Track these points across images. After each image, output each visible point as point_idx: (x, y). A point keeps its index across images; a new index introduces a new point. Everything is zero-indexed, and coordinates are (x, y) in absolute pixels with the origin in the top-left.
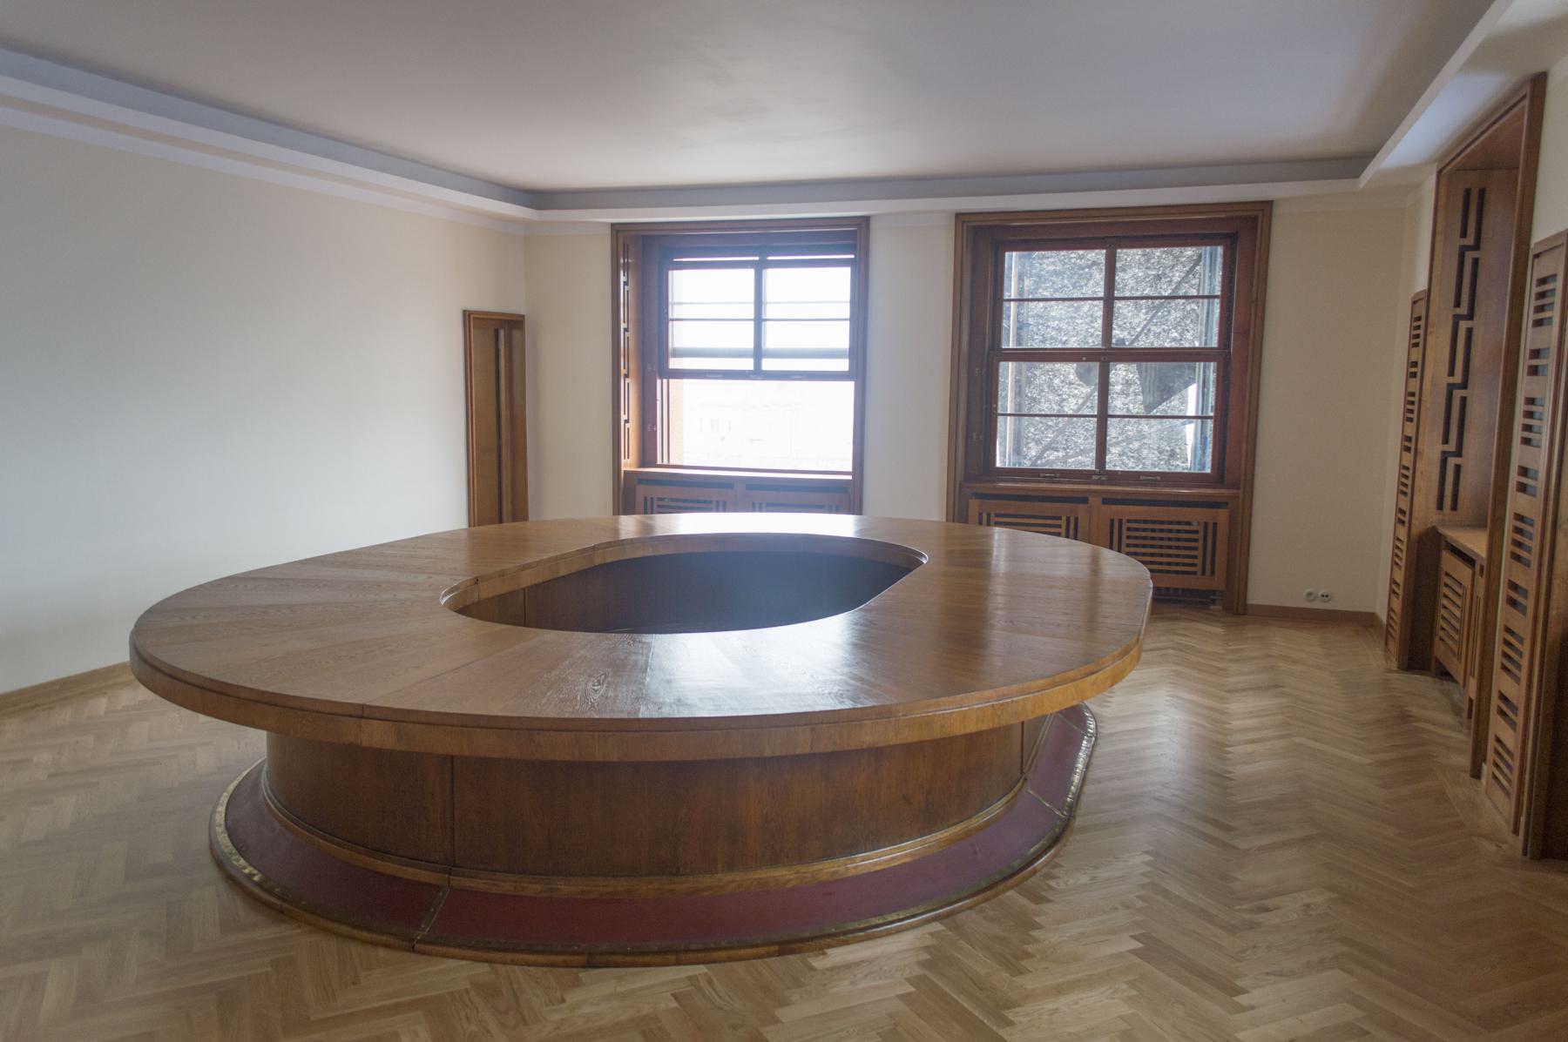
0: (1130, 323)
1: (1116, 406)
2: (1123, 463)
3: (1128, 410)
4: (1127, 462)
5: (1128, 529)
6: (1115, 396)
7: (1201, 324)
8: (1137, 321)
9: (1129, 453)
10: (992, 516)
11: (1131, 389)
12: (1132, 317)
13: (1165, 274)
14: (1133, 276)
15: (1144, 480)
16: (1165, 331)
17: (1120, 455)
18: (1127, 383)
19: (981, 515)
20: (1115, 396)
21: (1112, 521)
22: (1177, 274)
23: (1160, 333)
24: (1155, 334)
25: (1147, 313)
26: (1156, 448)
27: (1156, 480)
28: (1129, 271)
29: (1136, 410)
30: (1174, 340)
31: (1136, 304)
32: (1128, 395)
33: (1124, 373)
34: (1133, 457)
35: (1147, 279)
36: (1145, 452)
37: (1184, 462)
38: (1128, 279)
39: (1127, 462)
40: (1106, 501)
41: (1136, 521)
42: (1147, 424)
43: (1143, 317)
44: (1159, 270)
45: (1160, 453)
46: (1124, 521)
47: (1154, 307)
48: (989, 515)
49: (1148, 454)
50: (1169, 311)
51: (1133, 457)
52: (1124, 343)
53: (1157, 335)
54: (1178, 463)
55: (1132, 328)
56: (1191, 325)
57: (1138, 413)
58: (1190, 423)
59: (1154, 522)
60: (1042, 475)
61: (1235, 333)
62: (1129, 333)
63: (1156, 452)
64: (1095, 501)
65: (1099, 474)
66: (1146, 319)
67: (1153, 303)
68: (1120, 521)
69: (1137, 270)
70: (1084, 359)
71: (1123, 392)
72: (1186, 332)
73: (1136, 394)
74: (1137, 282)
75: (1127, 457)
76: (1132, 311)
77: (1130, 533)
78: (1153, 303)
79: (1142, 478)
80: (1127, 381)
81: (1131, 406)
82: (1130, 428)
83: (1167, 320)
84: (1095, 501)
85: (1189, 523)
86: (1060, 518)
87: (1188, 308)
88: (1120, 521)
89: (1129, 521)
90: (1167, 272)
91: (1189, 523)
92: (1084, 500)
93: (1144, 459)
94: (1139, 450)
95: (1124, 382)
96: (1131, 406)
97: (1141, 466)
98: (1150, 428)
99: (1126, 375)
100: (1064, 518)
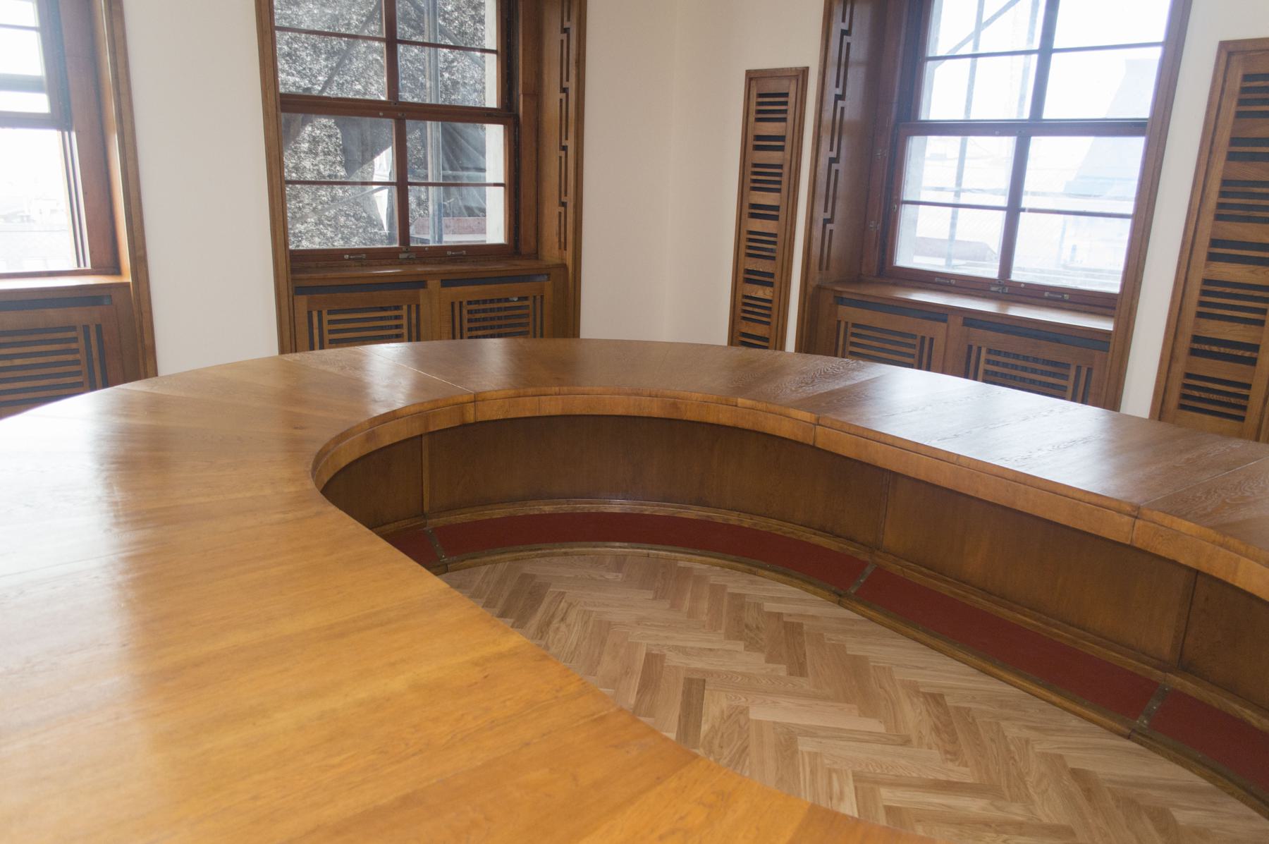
0: (310, 69)
1: (305, 167)
2: (321, 233)
3: (319, 172)
4: (325, 231)
5: (470, 312)
6: (302, 155)
7: (430, 80)
8: (317, 67)
9: (326, 222)
10: (325, 312)
11: (320, 148)
12: (312, 61)
13: (342, 15)
14: (308, 12)
15: (452, 256)
16: (348, 83)
17: (316, 224)
18: (314, 140)
19: (310, 314)
20: (302, 155)
21: (453, 304)
22: (355, 17)
23: (343, 84)
24: (338, 84)
25: (326, 59)
26: (352, 214)
27: (462, 255)
28: (302, 5)
29: (326, 173)
30: (358, 92)
31: (314, 46)
32: (317, 154)
34: (330, 225)
35: (324, 19)
36: (342, 219)
37: (380, 230)
38: (302, 15)
39: (325, 231)
40: (446, 283)
41: (477, 302)
42: (341, 189)
43: (323, 63)
44: (335, 10)
45: (357, 220)
46: (464, 303)
47: (334, 52)
48: (320, 313)
49: (345, 221)
50: (351, 60)
51: (330, 225)
52: (310, 92)
53: (341, 86)
54: (376, 230)
55: (313, 76)
56: (375, 78)
57: (330, 176)
58: (385, 188)
59: (492, 301)
60: (347, 257)
61: (524, 95)
62: (310, 81)
63: (353, 219)
64: (434, 284)
65: (405, 252)
66: (327, 66)
67: (332, 48)
68: (461, 303)
69: (311, 6)
70: (381, 114)
71: (310, 151)
72: (369, 85)
73: (327, 154)
74: (313, 20)
75: (324, 226)
76: (311, 55)
77: (471, 316)
78: (332, 48)
79: (449, 253)
80: (314, 138)
81: (322, 167)
82: (324, 193)
83: (349, 70)
84: (434, 284)
85: (507, 300)
86: (398, 308)
87: (370, 58)
88: (461, 303)
89: (469, 303)
90: (344, 13)
91: (507, 300)
92: (422, 284)
93: (342, 227)
94: (335, 218)
95: (312, 139)
96: (322, 167)
97: (340, 236)
98: (344, 192)
99: (313, 131)
100: (405, 307)
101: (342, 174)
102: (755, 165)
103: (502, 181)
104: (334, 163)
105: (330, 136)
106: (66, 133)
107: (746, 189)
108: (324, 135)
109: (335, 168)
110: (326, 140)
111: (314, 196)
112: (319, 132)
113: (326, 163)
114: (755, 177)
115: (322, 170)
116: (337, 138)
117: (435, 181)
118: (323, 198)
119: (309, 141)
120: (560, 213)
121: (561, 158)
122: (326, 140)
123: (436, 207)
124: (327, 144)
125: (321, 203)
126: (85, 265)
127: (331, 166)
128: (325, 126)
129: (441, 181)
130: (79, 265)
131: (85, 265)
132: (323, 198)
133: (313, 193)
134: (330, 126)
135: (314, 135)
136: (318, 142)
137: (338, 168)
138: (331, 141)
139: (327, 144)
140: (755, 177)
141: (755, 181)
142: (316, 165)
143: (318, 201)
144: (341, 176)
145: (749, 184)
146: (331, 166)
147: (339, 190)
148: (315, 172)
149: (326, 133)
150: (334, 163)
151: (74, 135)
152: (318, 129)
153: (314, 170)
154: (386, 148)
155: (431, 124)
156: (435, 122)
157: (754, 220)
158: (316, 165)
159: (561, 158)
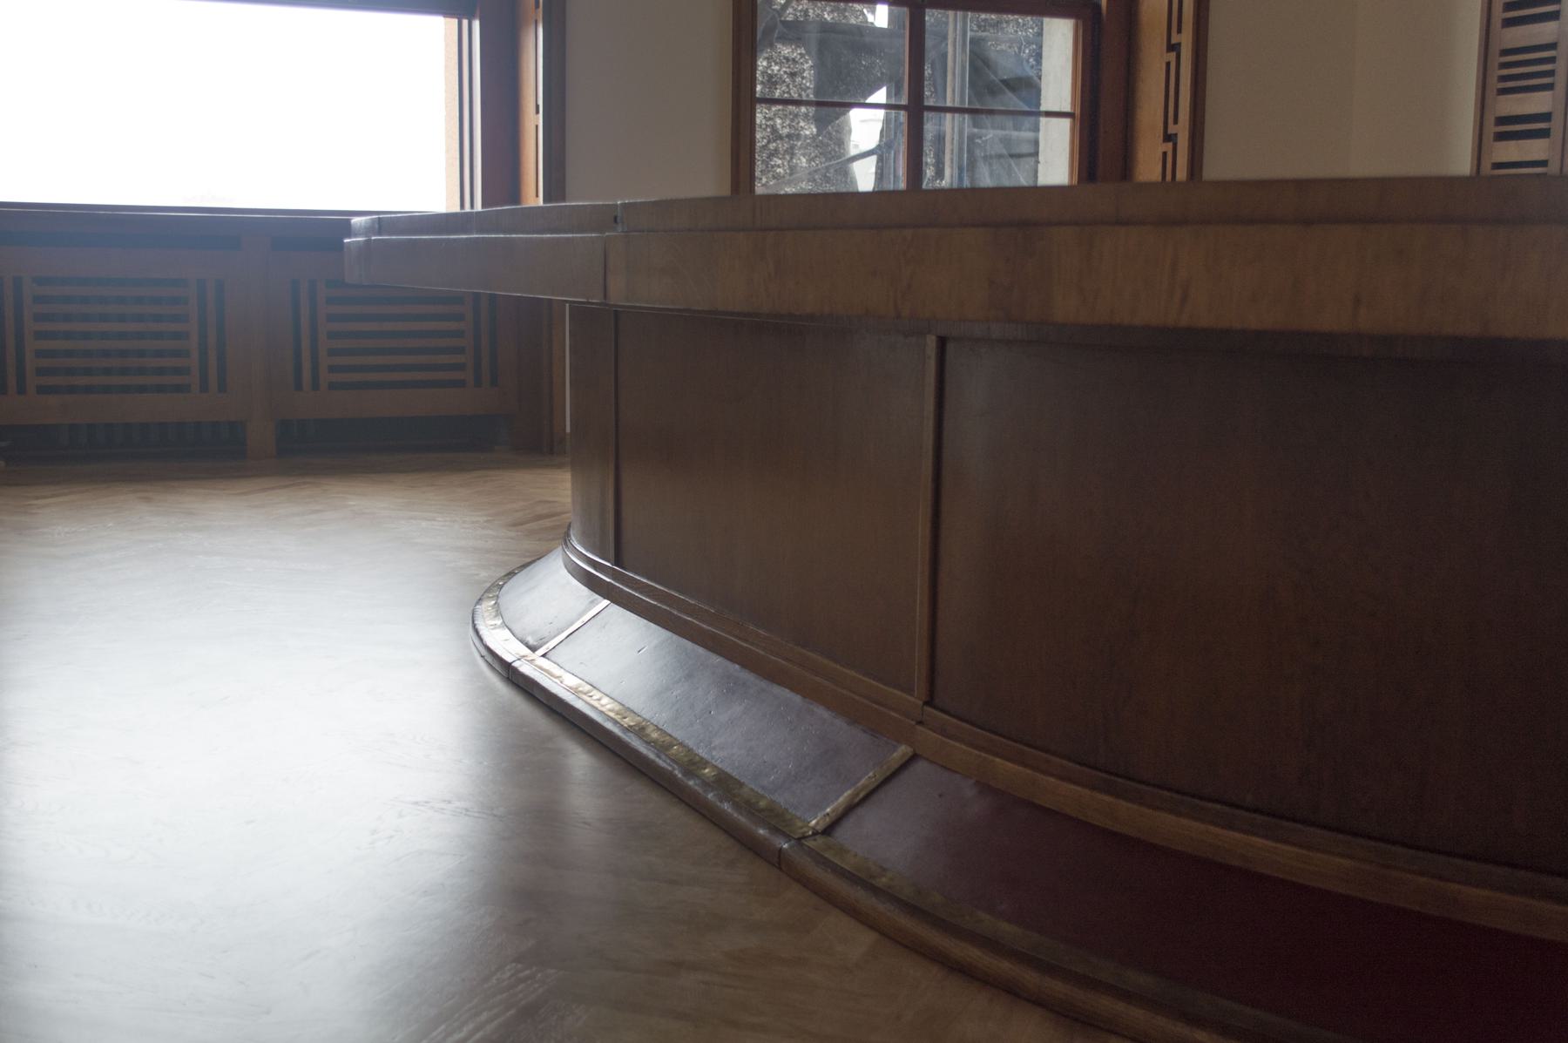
3: (774, 130)
18: (768, 81)
29: (786, 131)
33: (765, 63)
80: (771, 77)
81: (779, 121)
82: (780, 162)
95: (766, 78)
96: (779, 121)
101: (808, 133)
102: (1505, 52)
103: (1067, 108)
104: (796, 116)
105: (793, 75)
106: (465, 22)
107: (1491, 93)
108: (785, 72)
109: (799, 122)
110: (787, 80)
111: (764, 167)
112: (777, 68)
113: (786, 115)
114: (1505, 72)
115: (779, 126)
116: (803, 78)
117: (957, 105)
118: (778, 170)
119: (762, 83)
120: (1165, 154)
121: (1168, 64)
122: (787, 80)
123: (956, 171)
124: (788, 86)
125: (774, 177)
126: (472, 206)
127: (792, 120)
128: (787, 59)
129: (967, 106)
130: (462, 206)
131: (472, 206)
132: (778, 170)
133: (763, 161)
134: (794, 60)
135: (769, 72)
136: (776, 83)
137: (802, 124)
138: (794, 81)
139: (788, 86)
140: (1505, 72)
141: (1503, 79)
142: (770, 119)
143: (770, 175)
144: (806, 135)
145: (1494, 84)
146: (792, 120)
147: (802, 157)
148: (769, 130)
149: (788, 70)
150: (796, 116)
151: (476, 24)
152: (776, 64)
153: (767, 125)
154: (879, 88)
155: (956, 15)
156: (960, 14)
157: (1504, 143)
158: (770, 119)
159: (1168, 64)
